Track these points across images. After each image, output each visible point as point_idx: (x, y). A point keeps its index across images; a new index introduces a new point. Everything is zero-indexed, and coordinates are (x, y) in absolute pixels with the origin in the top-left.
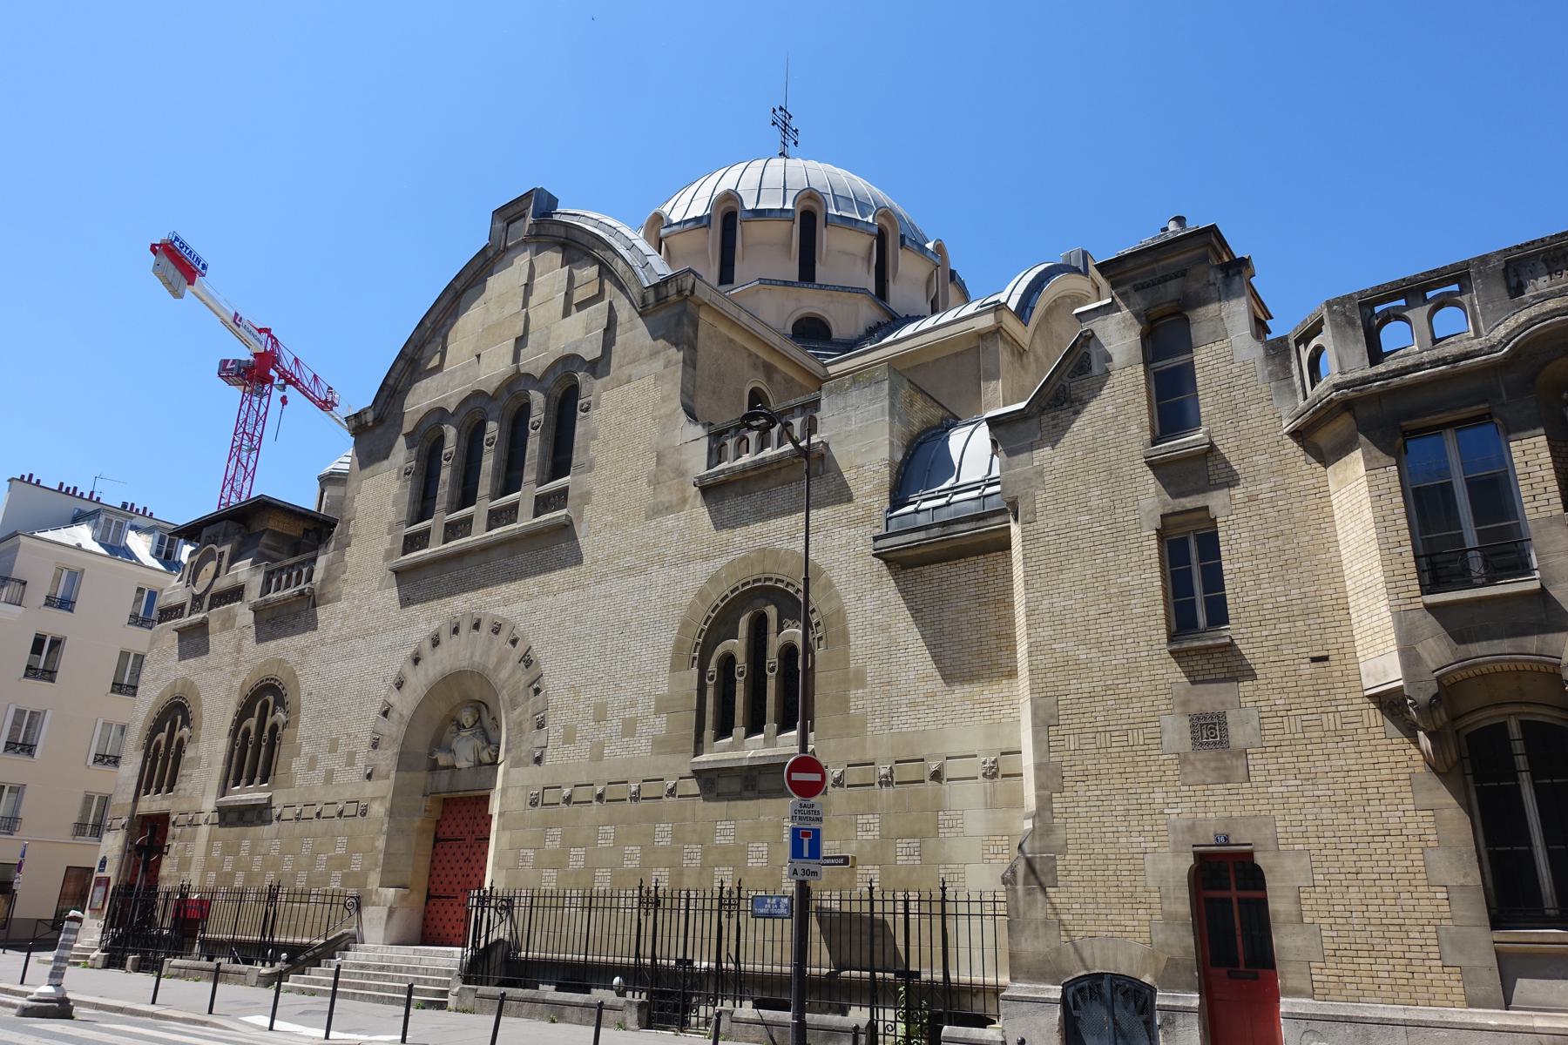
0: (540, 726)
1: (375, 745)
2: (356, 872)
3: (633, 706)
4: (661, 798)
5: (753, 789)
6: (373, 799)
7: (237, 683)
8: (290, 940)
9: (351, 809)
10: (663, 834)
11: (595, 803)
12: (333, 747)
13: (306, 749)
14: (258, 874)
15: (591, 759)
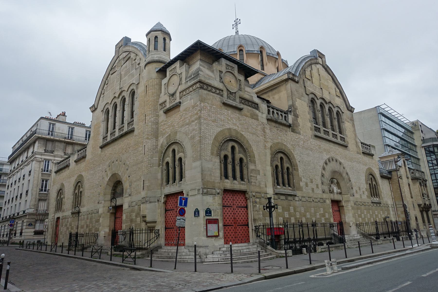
1: (322, 183)
2: (327, 218)
7: (269, 145)
12: (312, 182)
13: (303, 179)
14: (299, 218)
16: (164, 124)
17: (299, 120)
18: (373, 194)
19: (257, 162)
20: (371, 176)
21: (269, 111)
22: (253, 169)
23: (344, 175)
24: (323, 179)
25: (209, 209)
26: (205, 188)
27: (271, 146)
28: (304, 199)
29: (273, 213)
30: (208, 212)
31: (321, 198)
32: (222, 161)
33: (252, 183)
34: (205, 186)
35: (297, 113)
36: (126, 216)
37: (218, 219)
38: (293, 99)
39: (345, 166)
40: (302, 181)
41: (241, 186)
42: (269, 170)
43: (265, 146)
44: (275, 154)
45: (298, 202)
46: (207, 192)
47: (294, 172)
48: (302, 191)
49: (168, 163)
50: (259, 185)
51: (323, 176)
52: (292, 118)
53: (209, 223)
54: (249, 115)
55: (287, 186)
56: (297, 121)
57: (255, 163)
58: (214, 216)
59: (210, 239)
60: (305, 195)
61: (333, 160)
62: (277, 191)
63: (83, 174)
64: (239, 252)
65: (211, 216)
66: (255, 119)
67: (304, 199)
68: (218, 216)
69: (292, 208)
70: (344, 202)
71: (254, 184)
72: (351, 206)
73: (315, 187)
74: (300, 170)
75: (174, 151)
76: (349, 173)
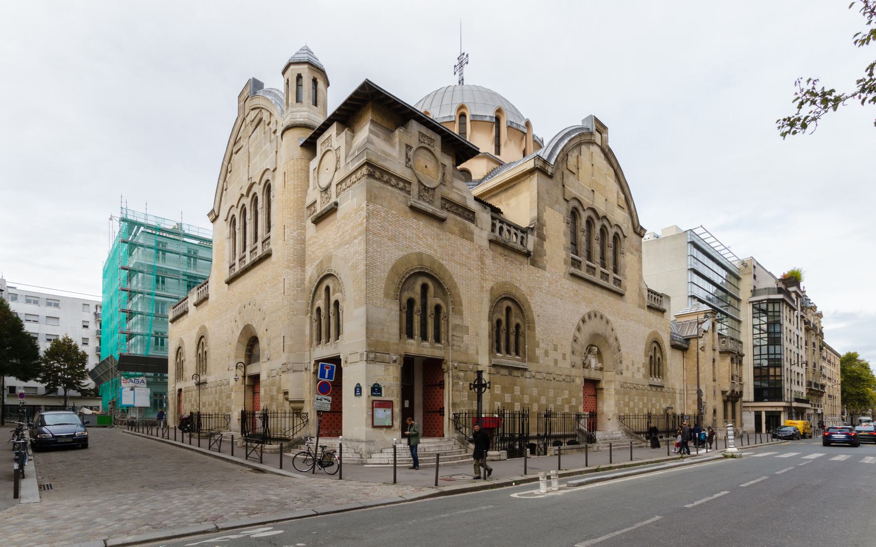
1: (573, 353)
2: (573, 406)
6: (576, 376)
7: (488, 285)
9: (568, 379)
12: (555, 349)
13: (542, 345)
16: (314, 243)
17: (546, 245)
18: (653, 373)
19: (465, 313)
20: (655, 345)
21: (493, 225)
22: (458, 325)
23: (611, 340)
24: (574, 345)
25: (378, 384)
26: (372, 352)
27: (492, 288)
28: (538, 376)
29: (483, 394)
30: (376, 389)
31: (569, 374)
32: (404, 308)
33: (455, 347)
34: (372, 349)
35: (545, 233)
36: (265, 391)
37: (392, 402)
38: (540, 208)
39: (614, 326)
40: (539, 347)
41: (436, 350)
42: (484, 328)
43: (482, 287)
44: (498, 302)
45: (528, 380)
46: (375, 358)
48: (537, 362)
49: (319, 309)
50: (466, 351)
51: (575, 341)
52: (535, 241)
53: (376, 407)
54: (457, 232)
55: (513, 353)
56: (543, 247)
57: (462, 315)
59: (377, 431)
60: (541, 370)
61: (596, 316)
63: (207, 324)
64: (423, 450)
65: (381, 395)
66: (467, 239)
67: (538, 376)
68: (392, 397)
69: (517, 390)
70: (606, 382)
71: (458, 348)
72: (615, 389)
73: (559, 357)
74: (538, 329)
75: (328, 288)
76: (620, 339)
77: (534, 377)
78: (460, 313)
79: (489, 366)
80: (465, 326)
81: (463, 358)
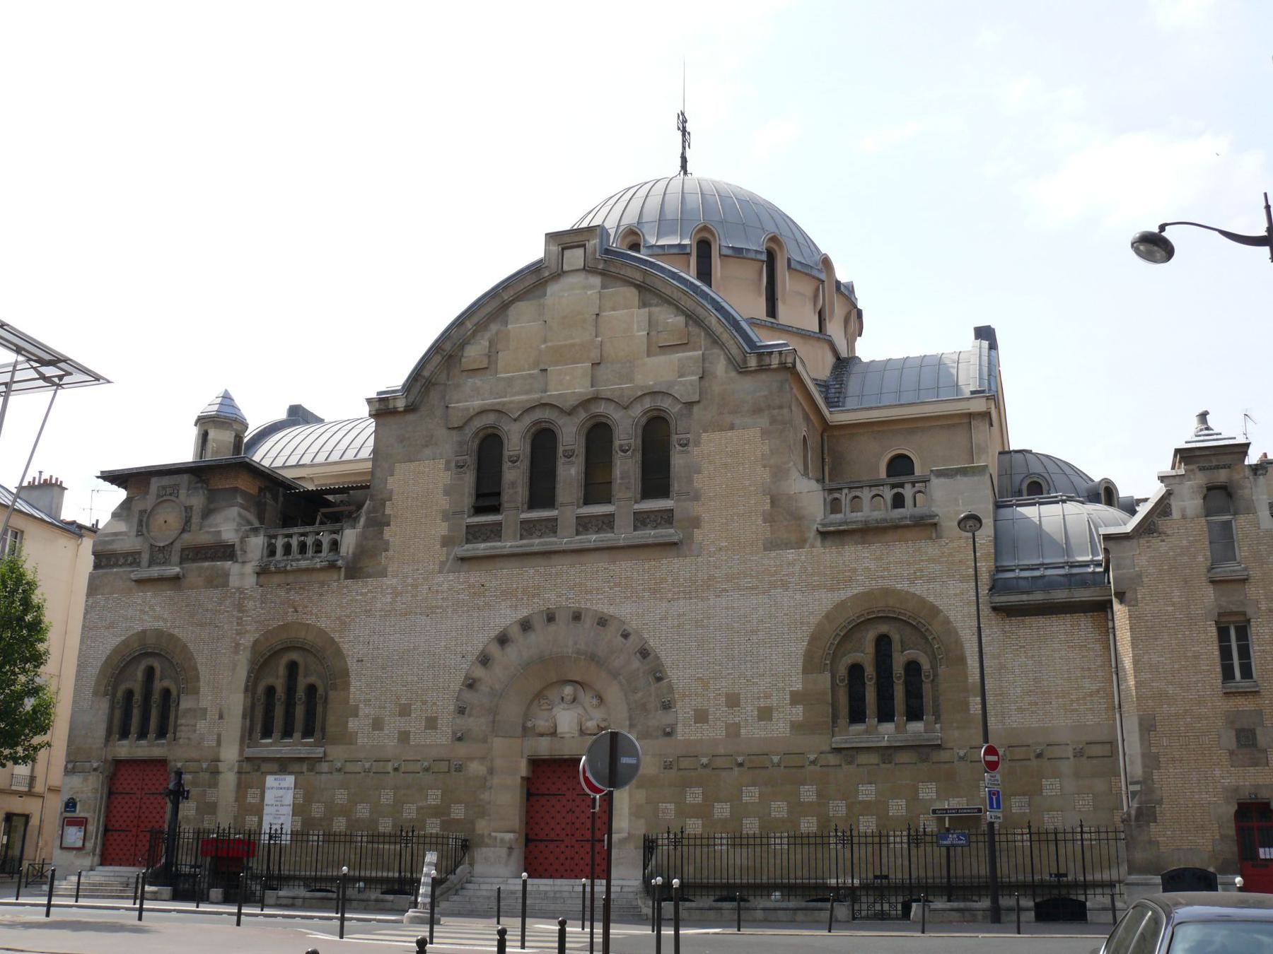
0: (667, 706)
1: (461, 711)
3: (766, 697)
4: (803, 767)
5: (890, 763)
6: (471, 759)
7: (247, 641)
8: (385, 874)
9: (443, 766)
10: (808, 793)
11: (736, 769)
13: (364, 710)
15: (727, 736)
19: (204, 689)
22: (190, 709)
27: (256, 642)
28: (350, 767)
30: (70, 805)
37: (86, 819)
42: (236, 702)
43: (238, 645)
45: (324, 777)
46: (73, 768)
47: (332, 694)
53: (67, 825)
58: (80, 812)
59: (64, 851)
62: (250, 752)
65: (75, 811)
68: (88, 812)
74: (357, 687)
77: (339, 770)
78: (196, 692)
79: (239, 761)
80: (201, 709)
81: (194, 755)
